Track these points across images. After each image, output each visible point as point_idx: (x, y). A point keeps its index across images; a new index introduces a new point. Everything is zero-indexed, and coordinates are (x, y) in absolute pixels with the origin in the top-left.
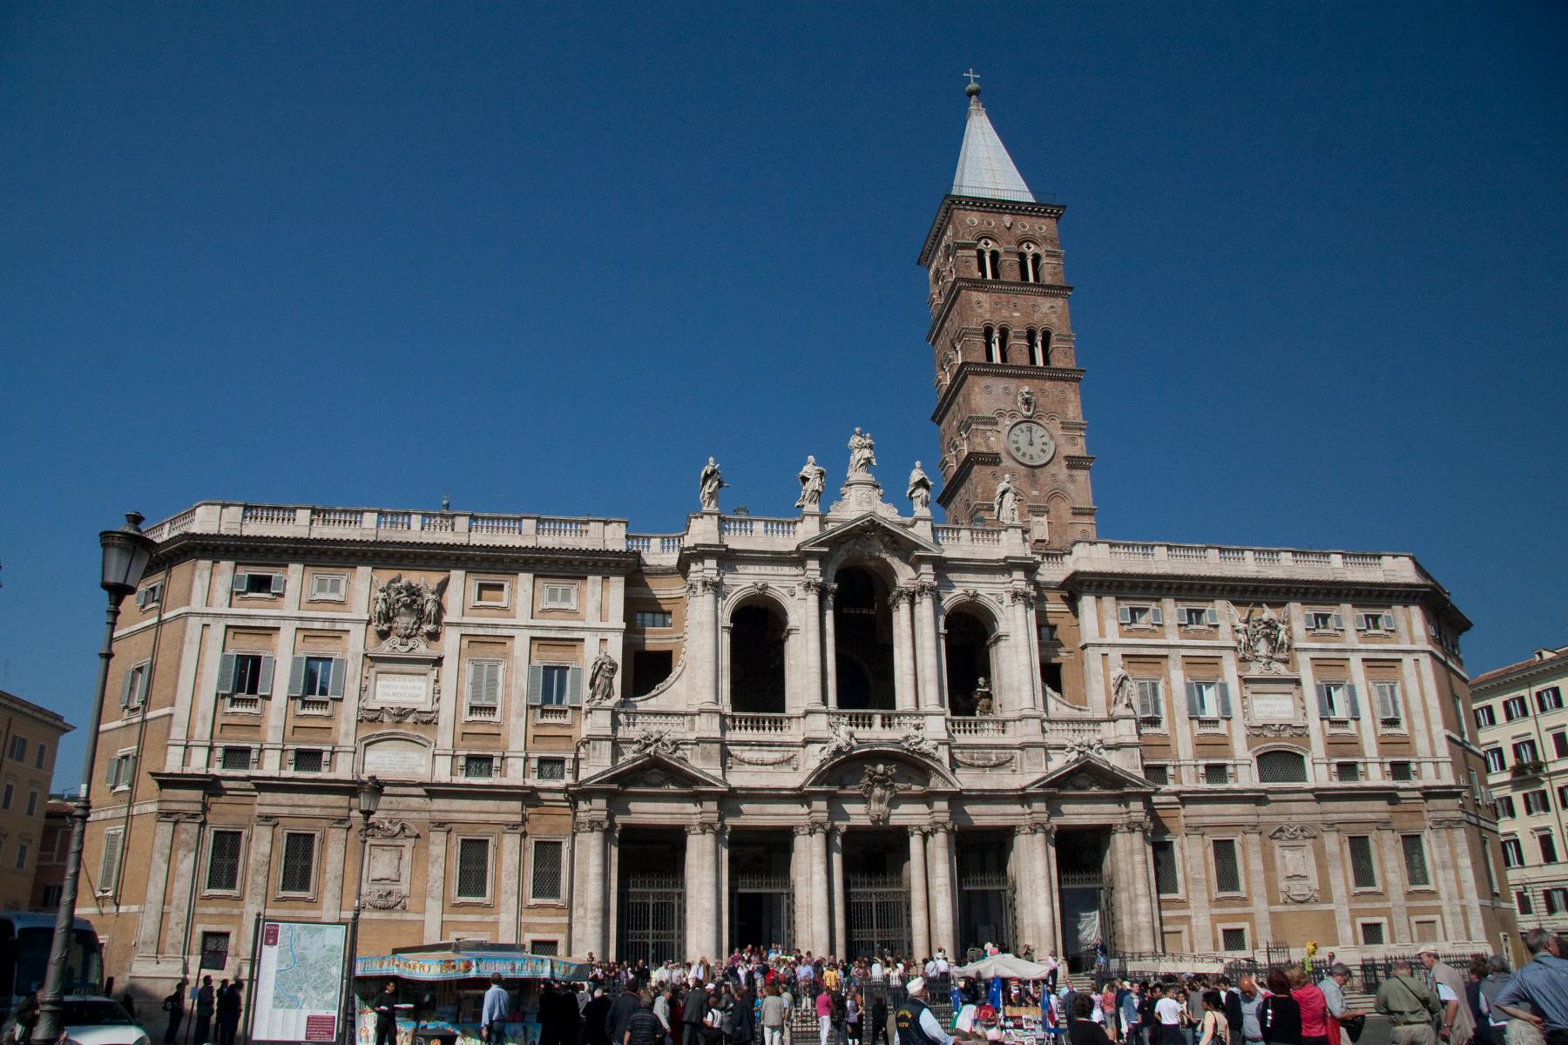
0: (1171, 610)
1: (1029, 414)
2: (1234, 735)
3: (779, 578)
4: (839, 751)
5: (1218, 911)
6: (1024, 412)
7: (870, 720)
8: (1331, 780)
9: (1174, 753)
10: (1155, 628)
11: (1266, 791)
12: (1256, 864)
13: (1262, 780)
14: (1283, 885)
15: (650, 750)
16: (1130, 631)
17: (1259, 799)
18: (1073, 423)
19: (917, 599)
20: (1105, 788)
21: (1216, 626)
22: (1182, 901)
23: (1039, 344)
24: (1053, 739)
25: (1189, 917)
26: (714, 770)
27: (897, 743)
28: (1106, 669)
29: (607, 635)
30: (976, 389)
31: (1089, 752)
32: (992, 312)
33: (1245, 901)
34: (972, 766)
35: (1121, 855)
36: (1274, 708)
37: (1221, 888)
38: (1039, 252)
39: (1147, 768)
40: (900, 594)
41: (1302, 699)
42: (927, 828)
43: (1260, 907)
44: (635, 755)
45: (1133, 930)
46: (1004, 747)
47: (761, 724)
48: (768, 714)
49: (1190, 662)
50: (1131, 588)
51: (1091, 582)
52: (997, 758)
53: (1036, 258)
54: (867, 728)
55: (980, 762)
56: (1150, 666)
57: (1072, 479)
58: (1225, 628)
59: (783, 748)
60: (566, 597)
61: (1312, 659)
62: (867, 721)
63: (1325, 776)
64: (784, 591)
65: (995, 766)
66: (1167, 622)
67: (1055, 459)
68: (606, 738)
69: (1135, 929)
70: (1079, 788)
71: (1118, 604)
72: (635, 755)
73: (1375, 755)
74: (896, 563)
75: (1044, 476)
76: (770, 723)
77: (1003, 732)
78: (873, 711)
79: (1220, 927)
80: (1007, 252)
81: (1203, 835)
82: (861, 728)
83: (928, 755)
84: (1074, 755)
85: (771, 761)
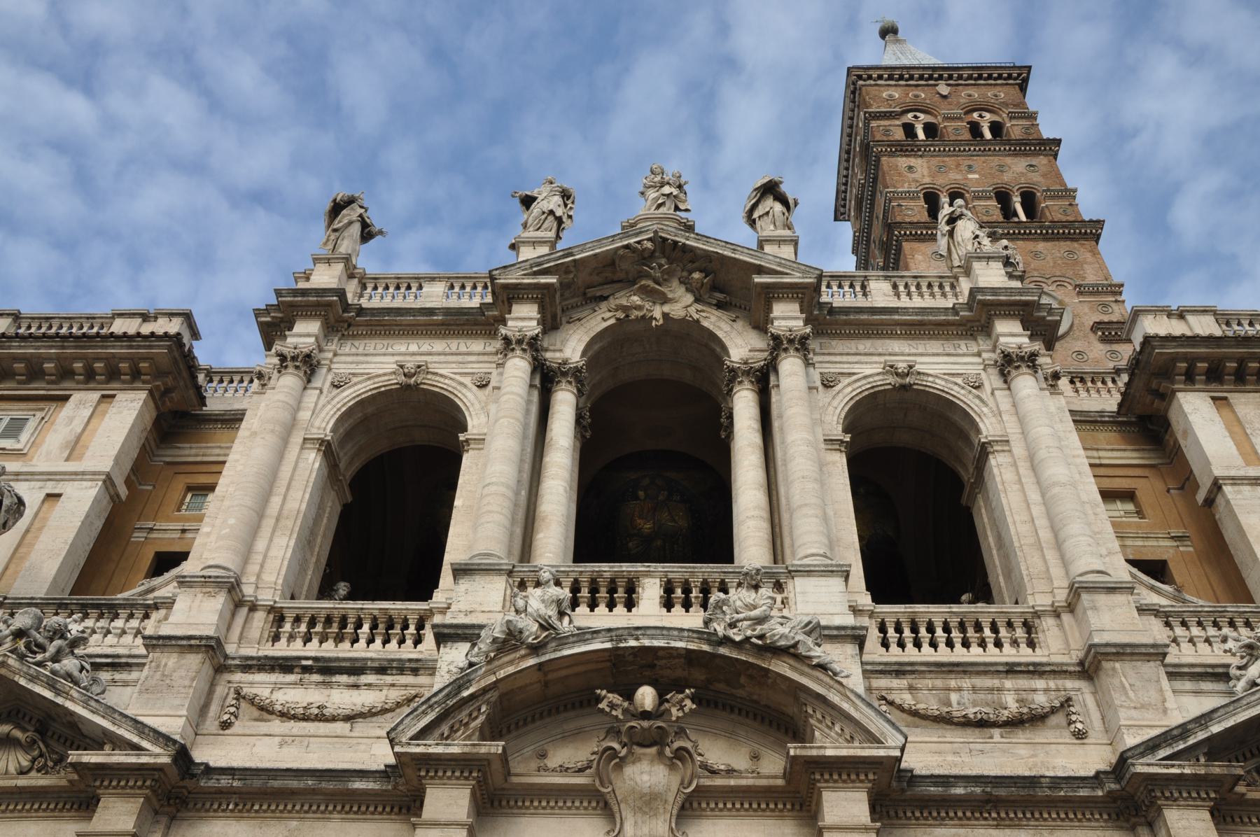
3: (460, 358)
4: (510, 641)
7: (631, 589)
18: (1093, 286)
29: (68, 489)
30: (919, 257)
32: (932, 176)
34: (944, 720)
38: (1000, 120)
40: (734, 374)
46: (1036, 670)
47: (350, 629)
48: (368, 605)
51: (1192, 360)
54: (620, 609)
55: (971, 712)
59: (389, 679)
60: (14, 428)
62: (620, 594)
64: (467, 380)
67: (1076, 333)
74: (716, 322)
76: (374, 627)
77: (1031, 644)
78: (640, 567)
80: (947, 118)
82: (602, 609)
83: (789, 652)
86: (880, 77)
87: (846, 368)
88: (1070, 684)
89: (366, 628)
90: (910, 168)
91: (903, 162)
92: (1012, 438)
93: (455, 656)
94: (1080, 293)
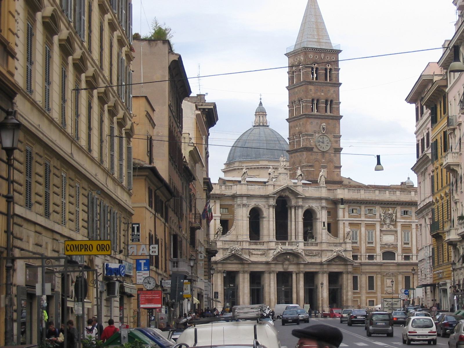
0: (363, 209)
1: (324, 132)
2: (377, 247)
5: (368, 295)
6: (322, 132)
7: (285, 242)
8: (402, 260)
9: (360, 251)
10: (358, 215)
11: (384, 263)
12: (379, 283)
13: (383, 260)
14: (386, 289)
15: (233, 252)
16: (351, 216)
17: (381, 265)
19: (297, 208)
20: (343, 262)
21: (375, 214)
22: (359, 292)
23: (329, 105)
24: (330, 248)
25: (360, 297)
26: (248, 257)
27: (292, 250)
28: (344, 227)
31: (340, 253)
32: (315, 93)
33: (375, 293)
34: (309, 255)
35: (345, 280)
36: (389, 239)
37: (369, 289)
39: (353, 256)
40: (293, 206)
41: (397, 237)
42: (297, 272)
43: (379, 295)
44: (230, 253)
45: (346, 300)
46: (317, 250)
49: (367, 225)
50: (353, 203)
52: (315, 253)
53: (330, 69)
55: (311, 254)
56: (355, 226)
57: (335, 156)
58: (378, 215)
61: (401, 224)
63: (401, 258)
64: (263, 206)
65: (314, 256)
66: (362, 213)
68: (222, 248)
69: (347, 300)
70: (336, 262)
71: (349, 207)
72: (230, 253)
73: (415, 253)
75: (327, 155)
79: (368, 300)
81: (366, 275)
83: (300, 254)
84: (335, 254)
85: (260, 254)
86: (310, 49)
87: (305, 205)
88: (319, 251)
89: (258, 244)
90: (311, 90)
91: (311, 87)
92: (321, 218)
93: (272, 251)
94: (334, 137)
